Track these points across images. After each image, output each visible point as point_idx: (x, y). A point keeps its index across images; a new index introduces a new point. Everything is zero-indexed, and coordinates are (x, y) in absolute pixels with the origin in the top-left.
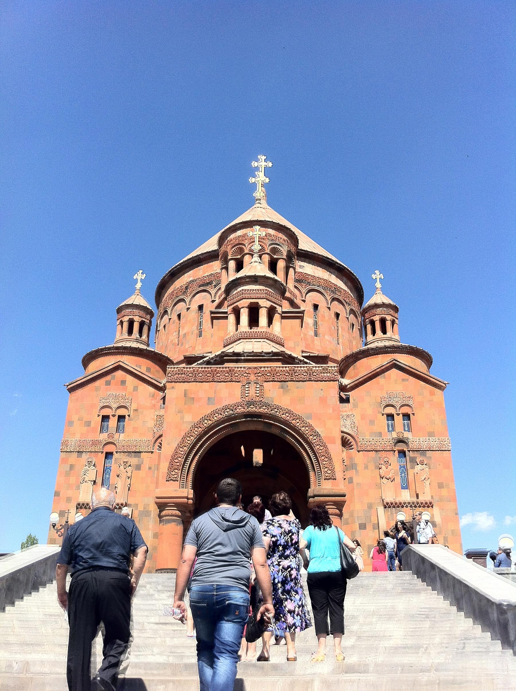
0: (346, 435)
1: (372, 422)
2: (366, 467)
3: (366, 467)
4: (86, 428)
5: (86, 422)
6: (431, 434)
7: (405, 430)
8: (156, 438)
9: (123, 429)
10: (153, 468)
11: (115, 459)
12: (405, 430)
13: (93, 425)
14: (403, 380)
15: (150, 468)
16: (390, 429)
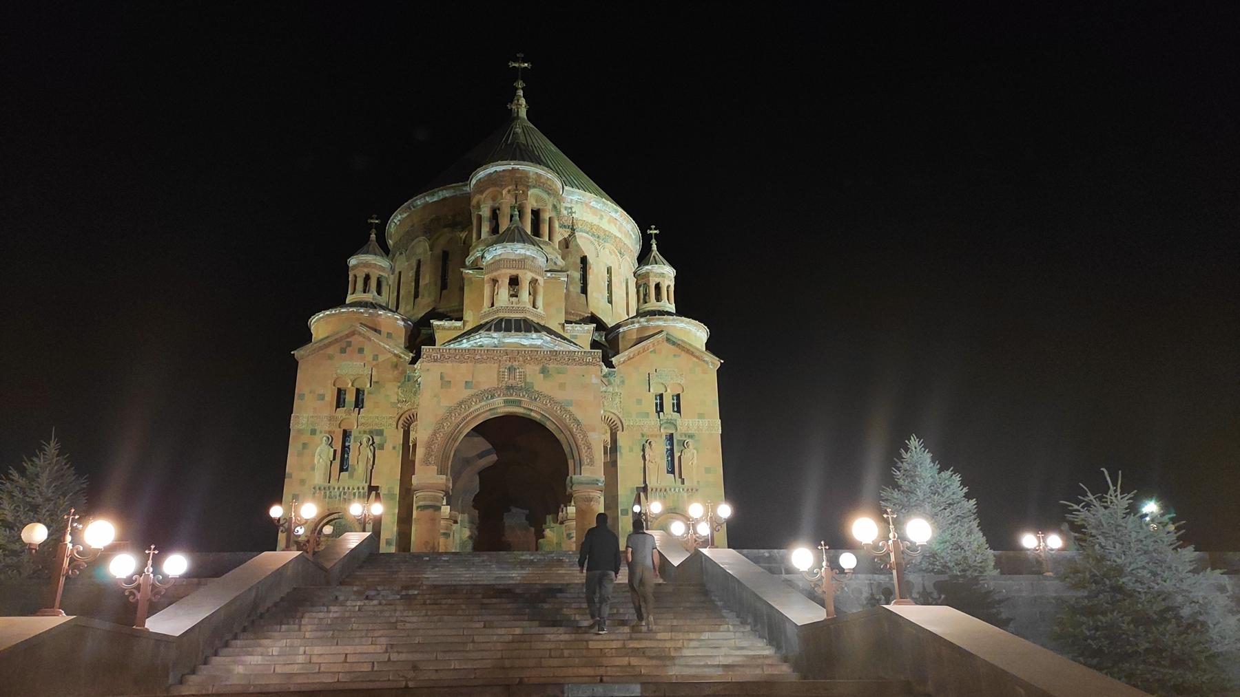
0: (612, 415)
1: (639, 402)
2: (631, 450)
3: (631, 450)
4: (319, 402)
5: (321, 395)
6: (701, 416)
7: (674, 411)
8: (400, 414)
9: (363, 403)
10: (397, 448)
11: (355, 437)
12: (674, 411)
13: (328, 398)
14: (675, 355)
15: (394, 448)
16: (658, 410)
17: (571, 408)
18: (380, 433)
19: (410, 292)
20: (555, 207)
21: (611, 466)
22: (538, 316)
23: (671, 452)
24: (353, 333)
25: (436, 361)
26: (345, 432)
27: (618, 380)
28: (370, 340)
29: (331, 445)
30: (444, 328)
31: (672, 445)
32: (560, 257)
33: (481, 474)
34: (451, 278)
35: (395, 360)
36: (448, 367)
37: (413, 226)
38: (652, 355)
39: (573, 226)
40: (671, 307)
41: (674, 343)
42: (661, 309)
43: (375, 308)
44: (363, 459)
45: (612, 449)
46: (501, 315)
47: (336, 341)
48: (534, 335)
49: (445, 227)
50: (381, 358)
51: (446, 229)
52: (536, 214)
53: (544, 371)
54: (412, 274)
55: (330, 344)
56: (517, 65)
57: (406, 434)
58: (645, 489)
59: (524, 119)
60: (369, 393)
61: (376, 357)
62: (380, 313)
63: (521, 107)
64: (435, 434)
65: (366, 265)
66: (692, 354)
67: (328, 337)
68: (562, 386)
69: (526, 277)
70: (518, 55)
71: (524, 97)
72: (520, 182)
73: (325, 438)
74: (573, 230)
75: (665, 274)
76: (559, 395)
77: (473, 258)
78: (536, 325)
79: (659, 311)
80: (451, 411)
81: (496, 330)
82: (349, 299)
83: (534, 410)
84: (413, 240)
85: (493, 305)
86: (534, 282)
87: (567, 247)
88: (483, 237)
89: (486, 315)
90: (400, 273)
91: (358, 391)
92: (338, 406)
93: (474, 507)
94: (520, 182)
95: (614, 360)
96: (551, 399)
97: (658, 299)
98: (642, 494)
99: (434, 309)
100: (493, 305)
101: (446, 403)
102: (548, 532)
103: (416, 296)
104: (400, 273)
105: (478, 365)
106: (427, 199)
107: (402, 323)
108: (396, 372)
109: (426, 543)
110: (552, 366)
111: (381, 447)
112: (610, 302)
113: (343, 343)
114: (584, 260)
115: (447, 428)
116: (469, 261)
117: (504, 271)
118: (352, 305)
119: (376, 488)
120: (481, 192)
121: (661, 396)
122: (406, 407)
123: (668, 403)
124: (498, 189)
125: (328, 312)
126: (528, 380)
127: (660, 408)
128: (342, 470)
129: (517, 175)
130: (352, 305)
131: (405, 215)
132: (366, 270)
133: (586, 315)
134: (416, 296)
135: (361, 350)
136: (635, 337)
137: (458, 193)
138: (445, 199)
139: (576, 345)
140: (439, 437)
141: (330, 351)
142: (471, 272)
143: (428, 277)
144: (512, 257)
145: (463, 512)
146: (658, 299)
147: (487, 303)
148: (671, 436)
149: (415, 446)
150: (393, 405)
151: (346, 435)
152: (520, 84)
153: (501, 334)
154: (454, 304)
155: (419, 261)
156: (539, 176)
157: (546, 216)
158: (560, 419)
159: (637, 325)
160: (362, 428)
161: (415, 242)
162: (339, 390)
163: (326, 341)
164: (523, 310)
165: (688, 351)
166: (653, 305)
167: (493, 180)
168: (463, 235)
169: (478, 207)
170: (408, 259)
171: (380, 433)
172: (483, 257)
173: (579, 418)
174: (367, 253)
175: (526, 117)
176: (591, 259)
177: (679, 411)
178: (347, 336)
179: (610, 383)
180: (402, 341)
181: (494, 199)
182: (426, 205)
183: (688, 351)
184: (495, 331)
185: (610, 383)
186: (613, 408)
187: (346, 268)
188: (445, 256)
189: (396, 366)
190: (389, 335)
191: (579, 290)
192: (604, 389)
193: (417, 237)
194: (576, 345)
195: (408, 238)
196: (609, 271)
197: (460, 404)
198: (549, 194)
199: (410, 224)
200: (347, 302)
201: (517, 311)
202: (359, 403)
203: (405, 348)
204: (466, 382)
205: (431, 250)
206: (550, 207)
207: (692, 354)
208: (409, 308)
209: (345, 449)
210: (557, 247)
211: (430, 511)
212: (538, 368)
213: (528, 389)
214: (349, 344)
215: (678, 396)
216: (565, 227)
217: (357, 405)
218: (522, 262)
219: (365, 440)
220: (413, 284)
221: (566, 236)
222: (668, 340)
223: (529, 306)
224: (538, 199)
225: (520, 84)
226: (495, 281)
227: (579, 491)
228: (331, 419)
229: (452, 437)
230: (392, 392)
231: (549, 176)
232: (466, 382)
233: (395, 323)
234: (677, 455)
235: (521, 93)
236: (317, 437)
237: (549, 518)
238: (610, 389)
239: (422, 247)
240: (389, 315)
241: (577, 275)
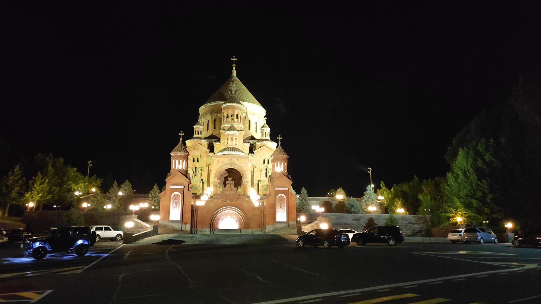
1: (260, 161)
2: (257, 172)
13: (191, 160)
14: (268, 151)
17: (243, 167)
18: (203, 168)
19: (206, 128)
20: (242, 113)
21: (253, 176)
22: (236, 146)
23: (266, 173)
24: (196, 145)
25: (216, 157)
26: (195, 167)
27: (254, 156)
28: (200, 147)
29: (193, 170)
30: (216, 144)
31: (266, 171)
32: (243, 126)
33: (225, 177)
34: (216, 126)
35: (205, 151)
36: (219, 159)
37: (206, 111)
38: (263, 151)
39: (247, 112)
40: (268, 138)
41: (268, 148)
42: (266, 139)
43: (201, 139)
44: (199, 173)
45: (253, 172)
46: (229, 146)
47: (193, 147)
48: (235, 152)
49: (215, 112)
50: (203, 151)
51: (215, 113)
52: (237, 116)
53: (237, 160)
54: (207, 124)
55: (191, 148)
56: (233, 59)
57: (208, 168)
58: (260, 181)
59: (235, 76)
60: (201, 159)
61: (201, 151)
62: (202, 140)
63: (234, 72)
64: (217, 172)
65: (198, 128)
66: (272, 150)
67: (191, 146)
68: (241, 163)
69: (234, 138)
70: (234, 56)
71: (235, 69)
72: (234, 108)
73: (191, 169)
74: (247, 113)
75: (268, 130)
76: (240, 165)
77: (222, 126)
78: (236, 149)
79: (265, 139)
80: (219, 167)
81: (228, 151)
82: (194, 136)
83: (236, 168)
84: (207, 115)
85: (227, 144)
86: (236, 138)
87: (245, 118)
88: (225, 121)
89: (226, 146)
90: (203, 123)
91: (198, 158)
92: (194, 162)
93: (223, 184)
94: (234, 108)
95: (254, 152)
96: (239, 166)
97: (265, 136)
98: (259, 182)
99: (212, 134)
100: (227, 144)
101: (218, 166)
102: (239, 190)
103: (208, 130)
104: (203, 123)
105: (225, 159)
106: (210, 104)
107: (207, 142)
108: (206, 154)
109: (215, 193)
110: (239, 159)
111: (203, 171)
112: (256, 131)
113: (194, 148)
114: (250, 121)
115: (219, 171)
116: (221, 127)
117: (229, 137)
118: (196, 138)
119: (202, 180)
120: (224, 110)
121: (265, 160)
122: (208, 162)
123: (266, 161)
124: (228, 110)
125: (190, 140)
126: (235, 161)
127: (264, 163)
128: (195, 176)
129: (233, 106)
130: (196, 138)
131: (204, 107)
132: (198, 129)
133: (250, 136)
134: (208, 130)
135: (198, 149)
136: (259, 146)
137: (218, 104)
138: (215, 105)
139: (244, 153)
140: (218, 173)
141: (191, 149)
142: (222, 131)
143: (211, 125)
144: (231, 134)
145: (221, 185)
146: (265, 136)
147: (226, 143)
148: (266, 169)
149: (210, 170)
150: (205, 162)
151: (196, 168)
152: (234, 65)
153: (229, 152)
154: (218, 133)
155: (208, 121)
156: (237, 106)
157: (239, 116)
158: (240, 169)
159: (260, 143)
160: (199, 167)
161: (207, 115)
162: (194, 158)
163: (190, 147)
164: (234, 145)
165: (271, 150)
166: (264, 138)
167: (227, 108)
168: (219, 115)
169: (224, 113)
170: (205, 120)
171: (203, 168)
172: (225, 133)
173: (244, 169)
174: (198, 125)
175: (235, 75)
176: (251, 121)
177: (268, 163)
178: (195, 146)
179: (253, 157)
180: (207, 146)
181: (227, 112)
182: (210, 106)
183: (271, 150)
184: (228, 151)
185: (253, 157)
186: (254, 163)
187: (194, 128)
188: (215, 120)
189: (206, 153)
190: (204, 145)
191: (248, 129)
192: (252, 158)
193: (208, 114)
194: (244, 153)
195: (205, 114)
196: (256, 123)
197: (221, 166)
198: (240, 110)
199: (206, 110)
200: (194, 137)
201: (233, 146)
202: (198, 161)
203: (208, 148)
204: (222, 162)
205: (211, 118)
206: (241, 113)
207: (272, 150)
208: (206, 132)
209: (195, 171)
210: (242, 123)
211: (215, 187)
212: (236, 159)
213: (234, 163)
214: (196, 148)
215: (268, 160)
216: (245, 113)
217: (198, 162)
218: (234, 135)
219: (200, 170)
220: (207, 127)
221: (245, 115)
222: (267, 147)
223: (235, 144)
224: (238, 112)
225: (234, 65)
226: (228, 138)
227: (243, 183)
228: (192, 164)
229: (219, 173)
230: (205, 159)
231: (240, 106)
232: (222, 162)
233: (205, 142)
234: (267, 173)
235: (234, 68)
236: (190, 169)
237: (239, 186)
238: (253, 158)
239: (209, 117)
240: (204, 141)
241: (248, 125)
